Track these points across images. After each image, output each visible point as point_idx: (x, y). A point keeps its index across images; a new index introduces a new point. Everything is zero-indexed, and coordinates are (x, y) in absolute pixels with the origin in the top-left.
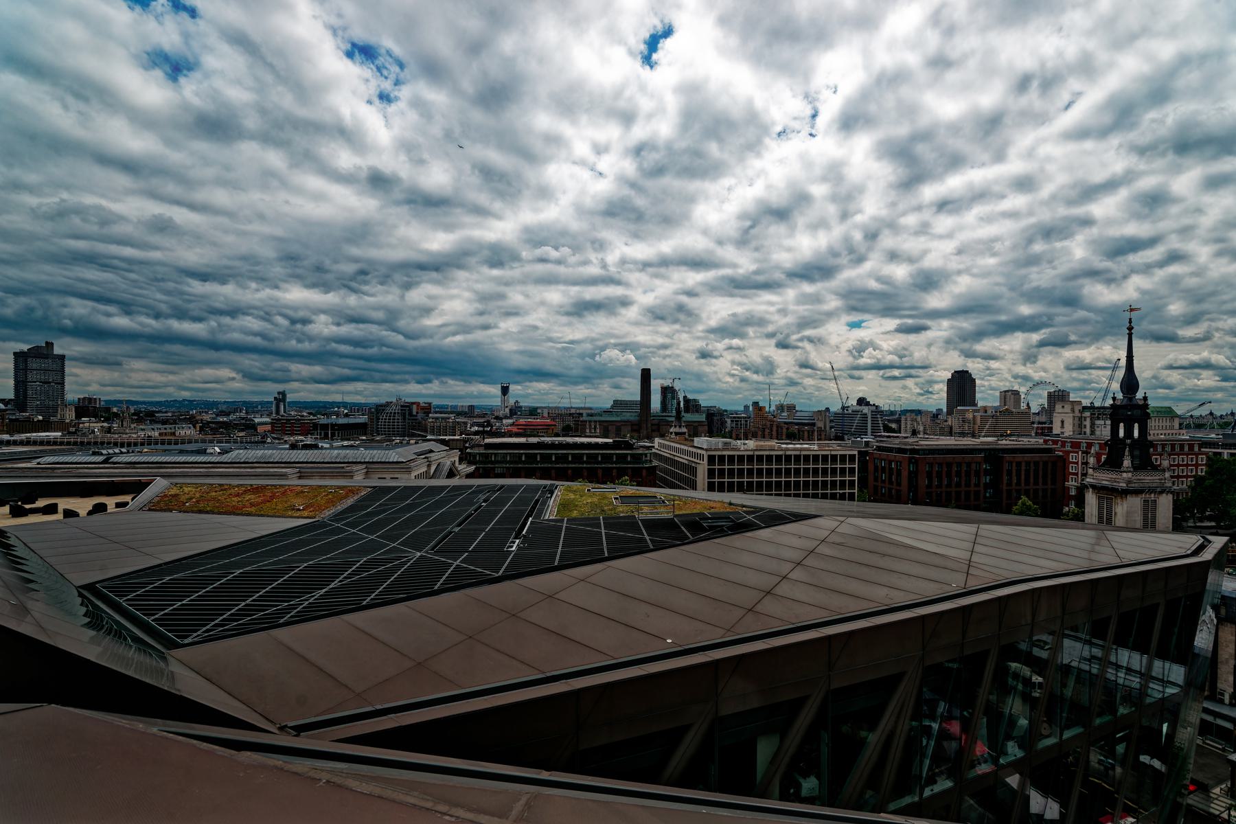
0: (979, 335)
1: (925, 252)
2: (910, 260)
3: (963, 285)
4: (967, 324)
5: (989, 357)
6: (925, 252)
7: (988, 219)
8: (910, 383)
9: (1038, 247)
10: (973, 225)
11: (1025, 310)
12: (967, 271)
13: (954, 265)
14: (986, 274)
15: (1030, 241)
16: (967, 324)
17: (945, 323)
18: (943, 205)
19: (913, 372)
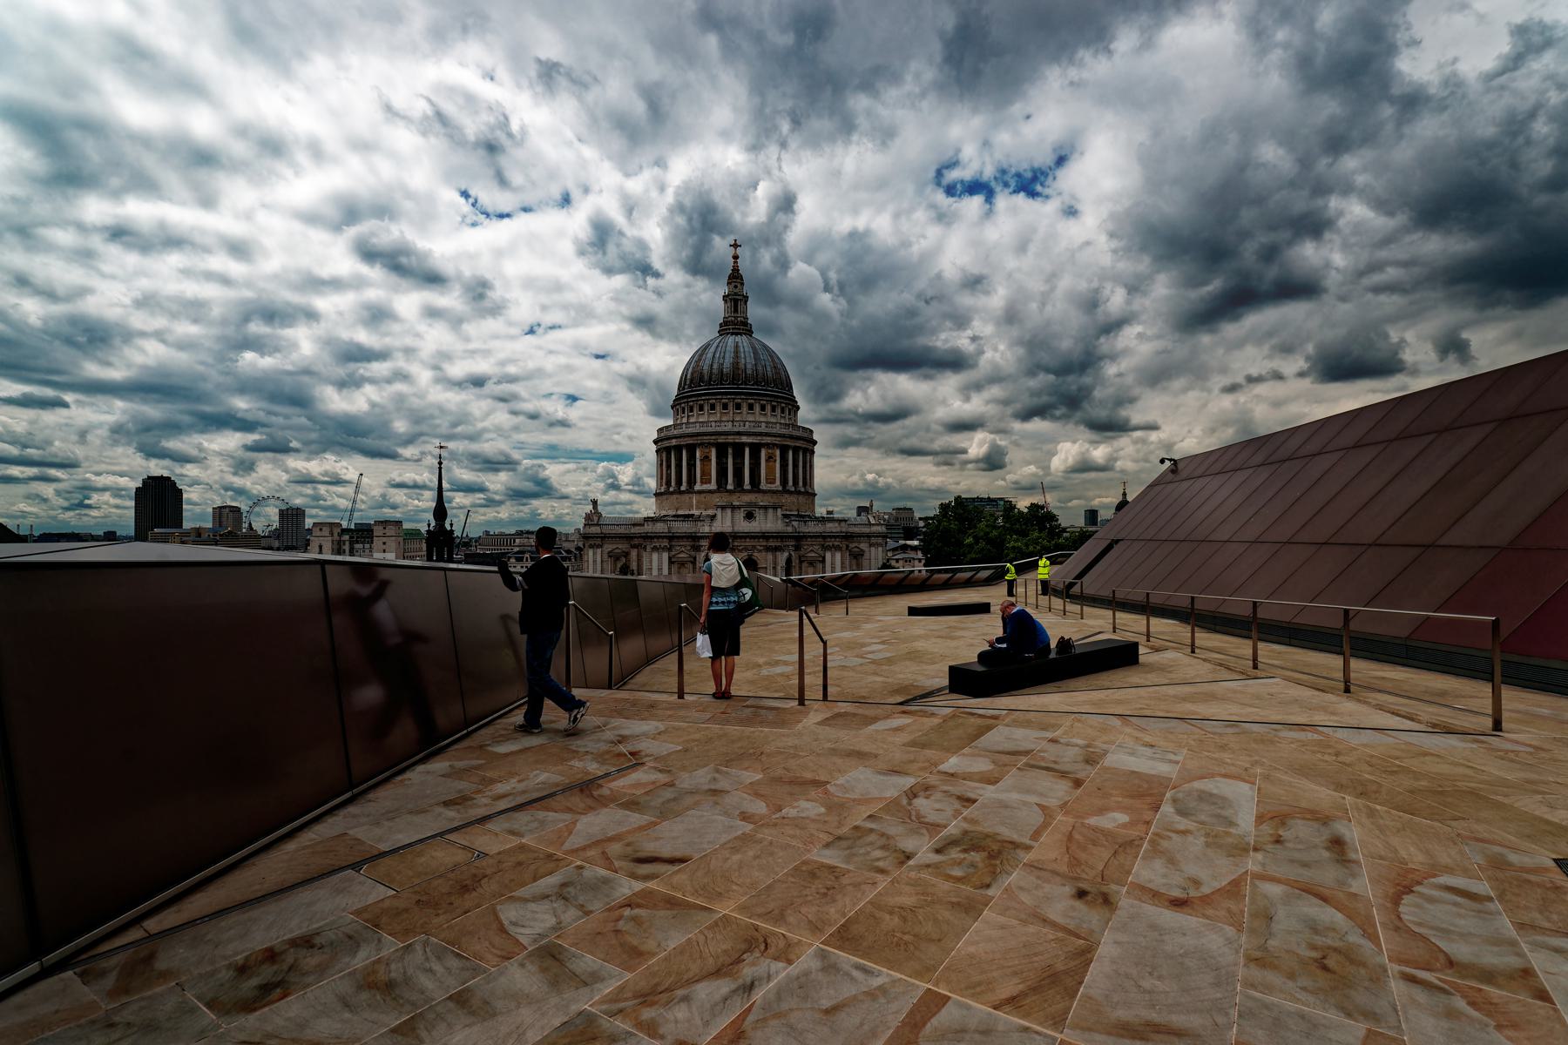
0: (173, 428)
1: (83, 292)
2: (49, 294)
3: (150, 354)
4: (153, 411)
5: (184, 459)
6: (83, 292)
7: (186, 273)
8: (48, 490)
9: (256, 328)
10: (166, 273)
11: (241, 404)
12: (159, 335)
13: (139, 320)
14: (183, 345)
15: (246, 319)
16: (153, 411)
17: (119, 404)
18: (119, 233)
19: (53, 472)
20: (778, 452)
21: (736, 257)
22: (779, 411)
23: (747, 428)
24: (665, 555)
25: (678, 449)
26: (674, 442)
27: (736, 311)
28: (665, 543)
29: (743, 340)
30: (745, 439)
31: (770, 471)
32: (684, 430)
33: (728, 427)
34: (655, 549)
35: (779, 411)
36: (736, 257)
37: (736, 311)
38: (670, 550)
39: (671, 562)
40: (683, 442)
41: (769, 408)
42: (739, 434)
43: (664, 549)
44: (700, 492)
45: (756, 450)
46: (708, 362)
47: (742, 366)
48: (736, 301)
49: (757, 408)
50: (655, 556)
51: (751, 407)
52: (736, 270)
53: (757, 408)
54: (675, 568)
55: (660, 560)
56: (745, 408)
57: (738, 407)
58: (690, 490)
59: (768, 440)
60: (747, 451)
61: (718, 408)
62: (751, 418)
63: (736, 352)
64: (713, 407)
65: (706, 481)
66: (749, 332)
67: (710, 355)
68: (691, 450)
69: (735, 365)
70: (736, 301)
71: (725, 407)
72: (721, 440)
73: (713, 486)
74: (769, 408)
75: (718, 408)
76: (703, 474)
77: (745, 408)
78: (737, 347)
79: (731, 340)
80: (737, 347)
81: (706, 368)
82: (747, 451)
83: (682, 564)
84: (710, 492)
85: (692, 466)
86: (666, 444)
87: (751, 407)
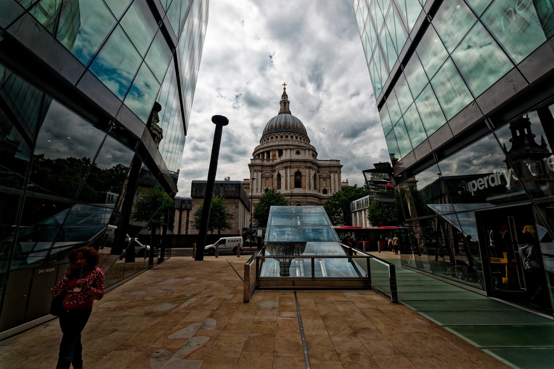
21: (285, 89)
22: (302, 140)
24: (260, 174)
25: (263, 153)
26: (261, 151)
27: (285, 106)
28: (260, 168)
29: (288, 115)
32: (265, 145)
33: (283, 143)
34: (255, 171)
36: (285, 89)
37: (285, 106)
38: (262, 171)
39: (262, 177)
40: (264, 150)
41: (299, 138)
43: (259, 171)
46: (275, 122)
47: (288, 122)
48: (285, 103)
49: (294, 137)
50: (255, 174)
51: (292, 137)
52: (285, 93)
53: (294, 137)
54: (264, 180)
55: (257, 176)
56: (289, 137)
57: (287, 137)
61: (279, 137)
64: (277, 137)
66: (290, 113)
67: (275, 120)
68: (268, 153)
69: (285, 123)
70: (285, 103)
71: (282, 137)
72: (280, 148)
75: (279, 137)
77: (289, 137)
79: (283, 115)
81: (274, 124)
83: (267, 178)
86: (258, 152)
87: (292, 137)
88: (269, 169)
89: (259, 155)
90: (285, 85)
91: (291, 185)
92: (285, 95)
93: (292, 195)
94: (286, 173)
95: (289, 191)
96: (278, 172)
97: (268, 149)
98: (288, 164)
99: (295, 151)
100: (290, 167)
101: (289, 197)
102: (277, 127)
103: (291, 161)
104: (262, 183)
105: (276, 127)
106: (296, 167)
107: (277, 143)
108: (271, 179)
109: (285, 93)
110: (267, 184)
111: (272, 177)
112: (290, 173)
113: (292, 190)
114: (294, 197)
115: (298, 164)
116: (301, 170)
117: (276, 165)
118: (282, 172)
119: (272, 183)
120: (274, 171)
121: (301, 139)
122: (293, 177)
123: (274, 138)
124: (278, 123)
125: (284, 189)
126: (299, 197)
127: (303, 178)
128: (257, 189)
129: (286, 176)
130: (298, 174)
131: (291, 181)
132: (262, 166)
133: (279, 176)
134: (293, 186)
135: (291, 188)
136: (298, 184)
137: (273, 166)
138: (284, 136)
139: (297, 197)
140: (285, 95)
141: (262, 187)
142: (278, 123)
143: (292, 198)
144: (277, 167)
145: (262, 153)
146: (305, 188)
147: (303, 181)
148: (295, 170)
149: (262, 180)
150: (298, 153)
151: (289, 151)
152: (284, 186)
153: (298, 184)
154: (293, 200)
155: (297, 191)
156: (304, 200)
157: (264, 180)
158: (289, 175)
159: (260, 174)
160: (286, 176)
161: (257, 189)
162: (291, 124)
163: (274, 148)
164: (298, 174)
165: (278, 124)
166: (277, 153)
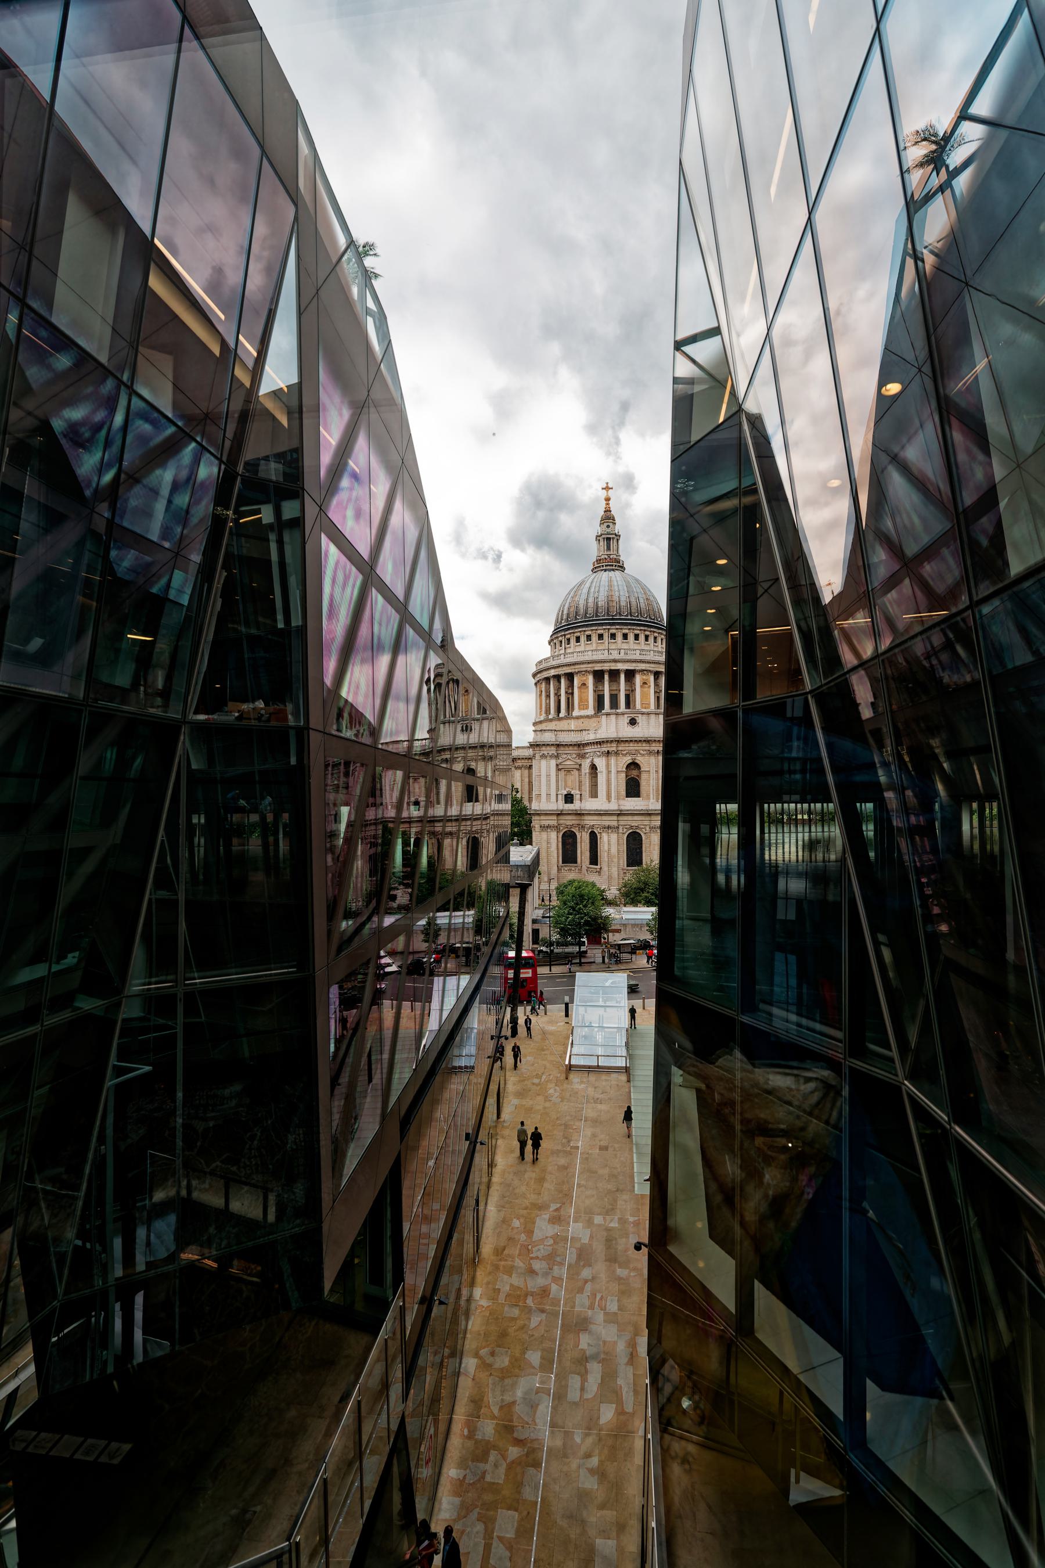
20: (652, 678)
21: (608, 499)
23: (622, 656)
24: (553, 763)
25: (557, 678)
26: (553, 672)
27: (609, 549)
28: (552, 751)
30: (620, 666)
31: (644, 696)
32: (562, 660)
33: (605, 656)
34: (543, 756)
35: (651, 639)
36: (608, 499)
37: (609, 549)
38: (557, 757)
39: (558, 770)
41: (642, 637)
42: (615, 661)
44: (578, 718)
45: (630, 675)
46: (584, 596)
47: (616, 598)
48: (608, 539)
50: (544, 762)
51: (625, 636)
52: (608, 511)
54: (562, 774)
55: (548, 767)
58: (569, 716)
59: (643, 666)
60: (622, 676)
61: (595, 638)
62: (625, 646)
63: (610, 586)
65: (584, 706)
66: (622, 568)
67: (585, 591)
68: (570, 677)
71: (601, 637)
72: (598, 667)
73: (591, 711)
74: (642, 637)
75: (595, 638)
76: (580, 700)
78: (610, 586)
79: (605, 576)
80: (610, 581)
81: (582, 603)
82: (622, 676)
83: (569, 771)
84: (588, 717)
85: (570, 694)
86: (545, 674)
88: (573, 751)
89: (547, 680)
90: (607, 488)
91: (618, 792)
92: (608, 518)
93: (620, 814)
94: (608, 766)
95: (613, 806)
96: (592, 762)
97: (568, 670)
98: (613, 748)
99: (626, 719)
100: (617, 753)
101: (615, 818)
102: (590, 611)
103: (619, 741)
104: (557, 781)
105: (586, 613)
106: (629, 753)
107: (588, 657)
108: (576, 772)
109: (608, 511)
110: (569, 783)
111: (579, 770)
112: (617, 765)
113: (621, 802)
114: (625, 818)
115: (632, 747)
116: (639, 760)
117: (587, 744)
118: (600, 763)
119: (580, 782)
120: (583, 756)
121: (647, 638)
122: (623, 775)
123: (583, 639)
124: (591, 600)
125: (605, 799)
126: (636, 818)
127: (644, 776)
128: (548, 795)
129: (609, 772)
130: (634, 765)
131: (619, 783)
132: (558, 745)
133: (594, 767)
134: (624, 793)
135: (618, 799)
136: (633, 789)
137: (579, 745)
138: (606, 636)
139: (630, 818)
140: (608, 518)
141: (557, 789)
142: (591, 600)
143: (621, 818)
144: (588, 749)
145: (554, 676)
146: (648, 798)
147: (643, 783)
148: (628, 759)
149: (557, 775)
150: (633, 722)
151: (613, 717)
152: (605, 793)
153: (633, 789)
154: (621, 823)
155: (632, 804)
156: (646, 823)
157: (562, 774)
158: (613, 770)
159: (553, 763)
160: (609, 772)
161: (548, 795)
162: (623, 604)
163: (583, 667)
164: (634, 765)
165: (591, 604)
166: (590, 680)
